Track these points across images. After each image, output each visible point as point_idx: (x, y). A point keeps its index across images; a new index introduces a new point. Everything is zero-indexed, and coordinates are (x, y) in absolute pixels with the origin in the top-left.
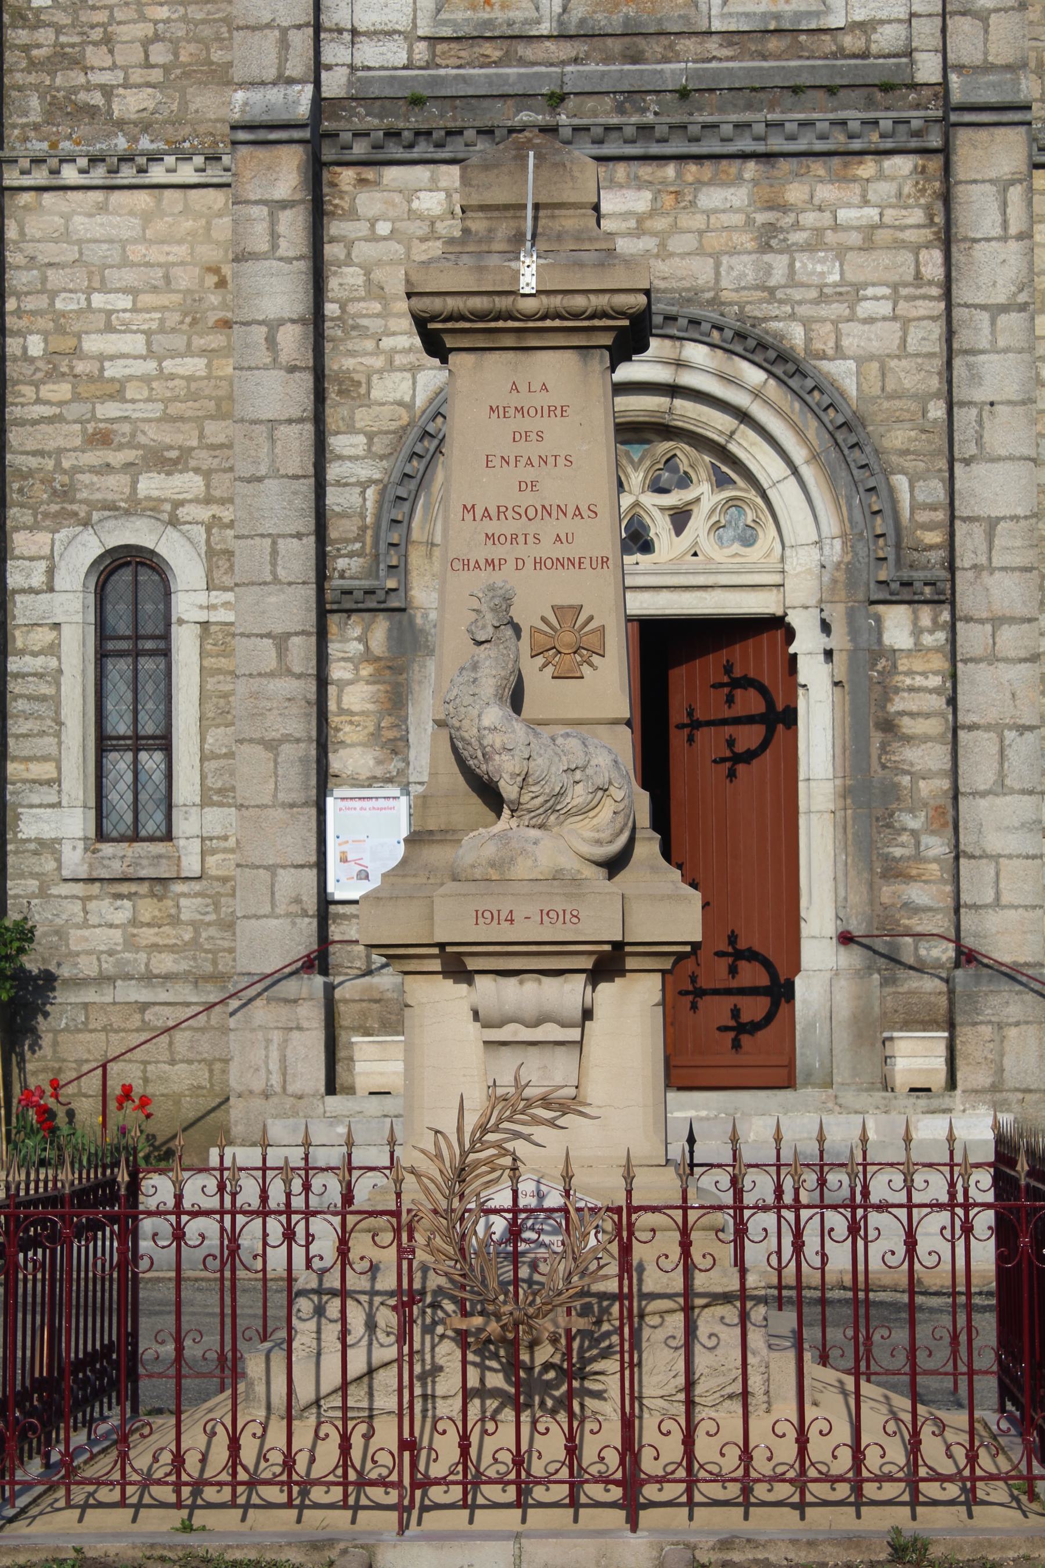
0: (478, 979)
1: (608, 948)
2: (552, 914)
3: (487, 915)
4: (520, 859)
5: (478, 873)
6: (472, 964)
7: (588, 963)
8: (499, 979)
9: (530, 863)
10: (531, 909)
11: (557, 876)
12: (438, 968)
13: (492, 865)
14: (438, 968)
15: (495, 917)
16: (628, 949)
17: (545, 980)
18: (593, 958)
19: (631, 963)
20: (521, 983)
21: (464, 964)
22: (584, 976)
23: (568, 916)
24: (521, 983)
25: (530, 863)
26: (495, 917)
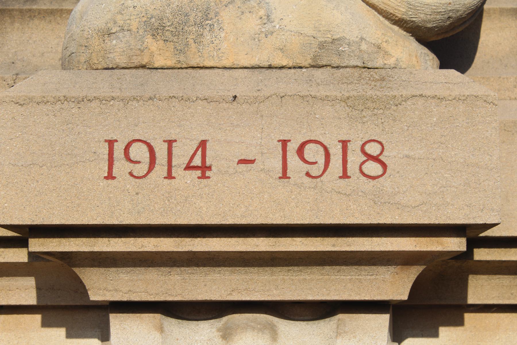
0: (117, 322)
1: (456, 244)
2: (313, 152)
3: (139, 152)
4: (227, 15)
5: (118, 50)
6: (102, 286)
7: (395, 286)
8: (172, 325)
9: (252, 24)
10: (259, 139)
11: (323, 58)
12: (30, 298)
13: (157, 29)
14: (30, 298)
15: (159, 159)
16: (481, 254)
17: (287, 328)
18: (414, 273)
19: (480, 290)
20: (226, 334)
21: (82, 290)
22: (383, 320)
23: (355, 158)
24: (226, 334)
25: (252, 24)
26: (159, 159)
